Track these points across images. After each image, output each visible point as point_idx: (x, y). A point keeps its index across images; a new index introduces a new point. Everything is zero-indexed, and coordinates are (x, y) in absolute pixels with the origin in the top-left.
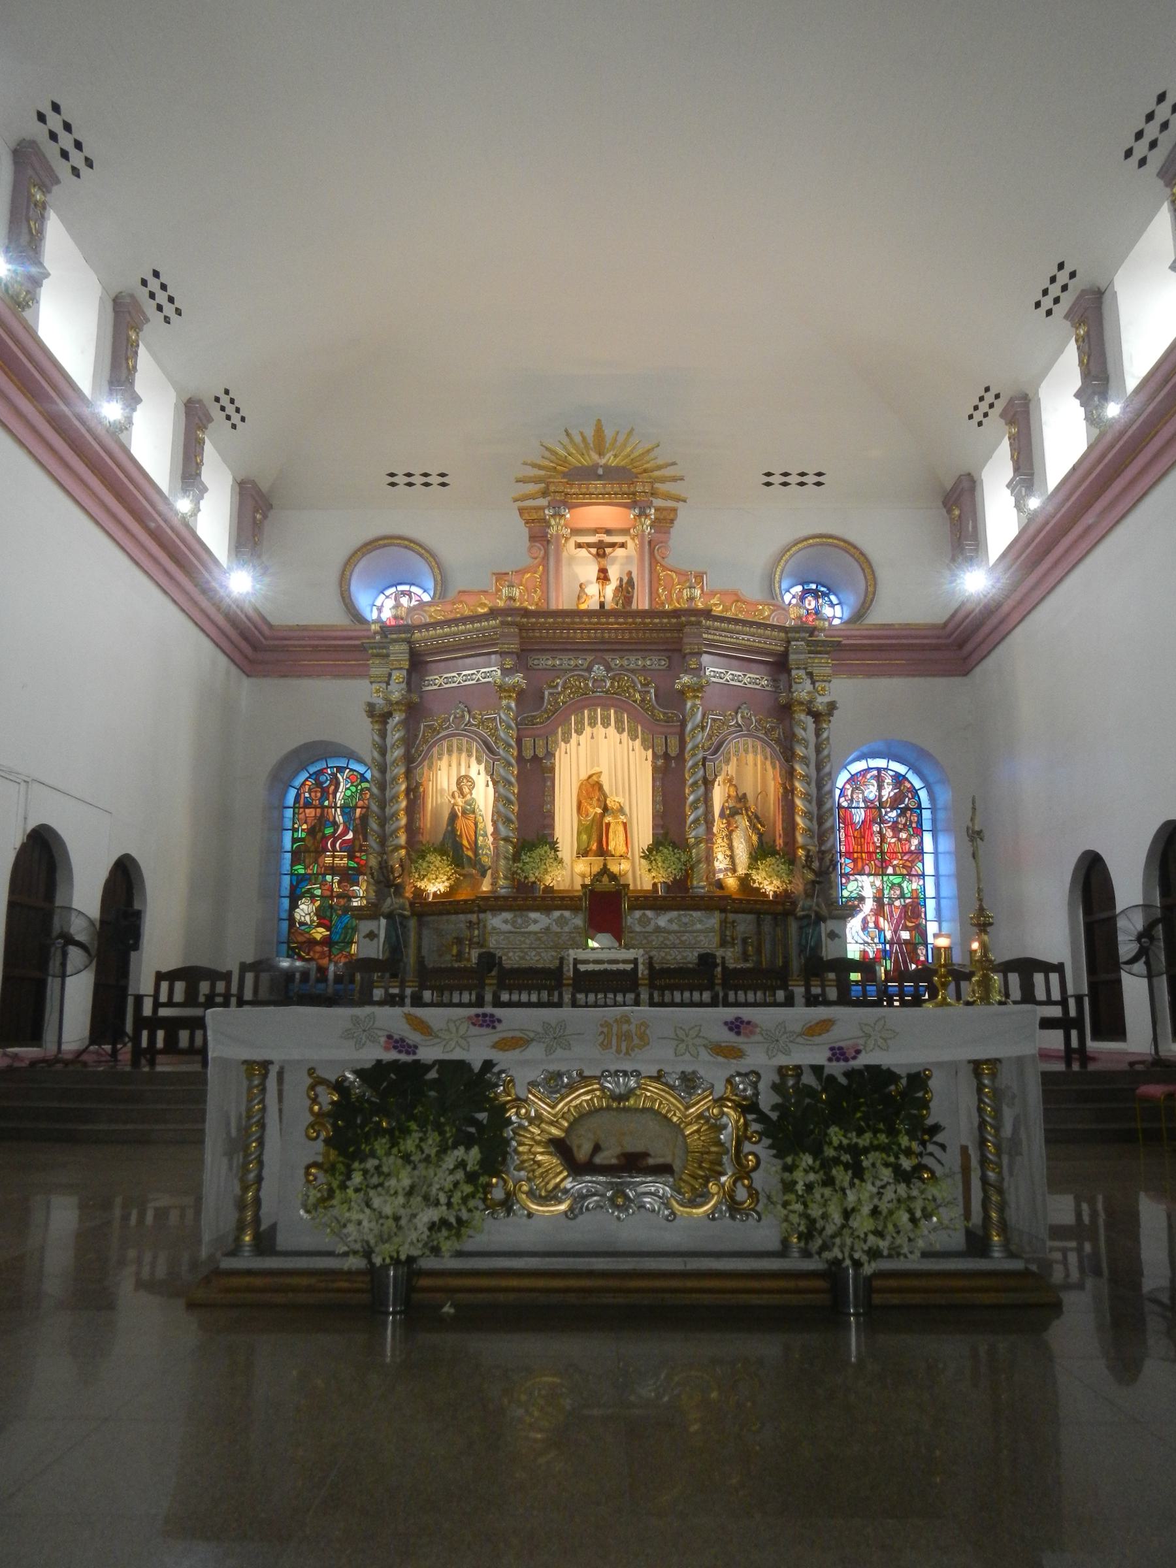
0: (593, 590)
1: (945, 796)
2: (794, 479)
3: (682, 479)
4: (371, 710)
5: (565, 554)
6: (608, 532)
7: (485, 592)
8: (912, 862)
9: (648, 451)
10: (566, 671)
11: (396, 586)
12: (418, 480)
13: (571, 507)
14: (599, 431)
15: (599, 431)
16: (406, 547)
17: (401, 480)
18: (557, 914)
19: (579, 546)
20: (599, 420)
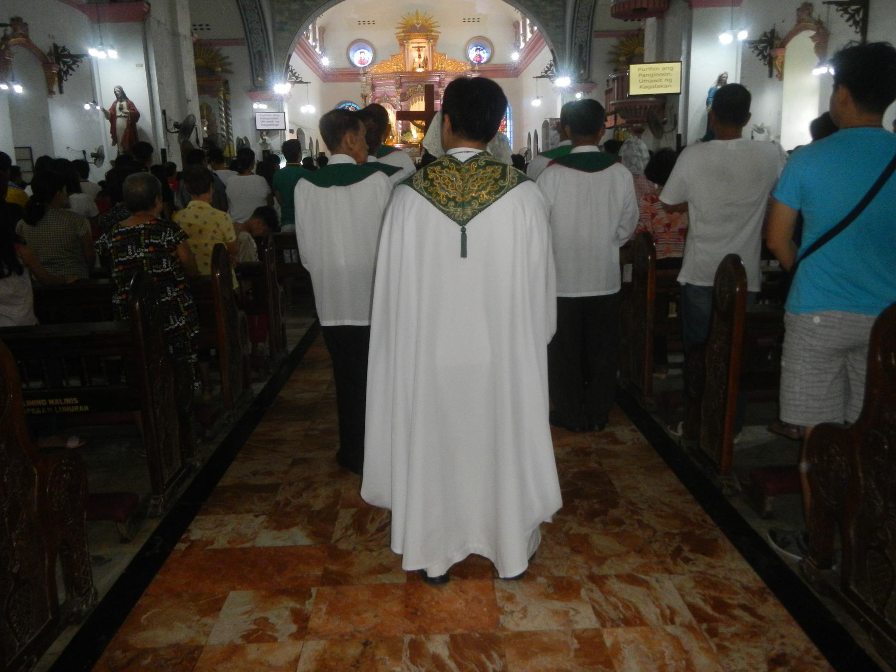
0: (417, 60)
1: (511, 111)
2: (471, 20)
3: (440, 26)
4: (362, 94)
5: (409, 50)
6: (421, 43)
7: (388, 61)
8: (504, 128)
9: (431, 18)
10: (411, 87)
11: (360, 49)
12: (367, 23)
13: (410, 39)
14: (417, 12)
15: (417, 12)
16: (364, 42)
17: (362, 23)
18: (412, 148)
19: (413, 47)
20: (417, 10)
